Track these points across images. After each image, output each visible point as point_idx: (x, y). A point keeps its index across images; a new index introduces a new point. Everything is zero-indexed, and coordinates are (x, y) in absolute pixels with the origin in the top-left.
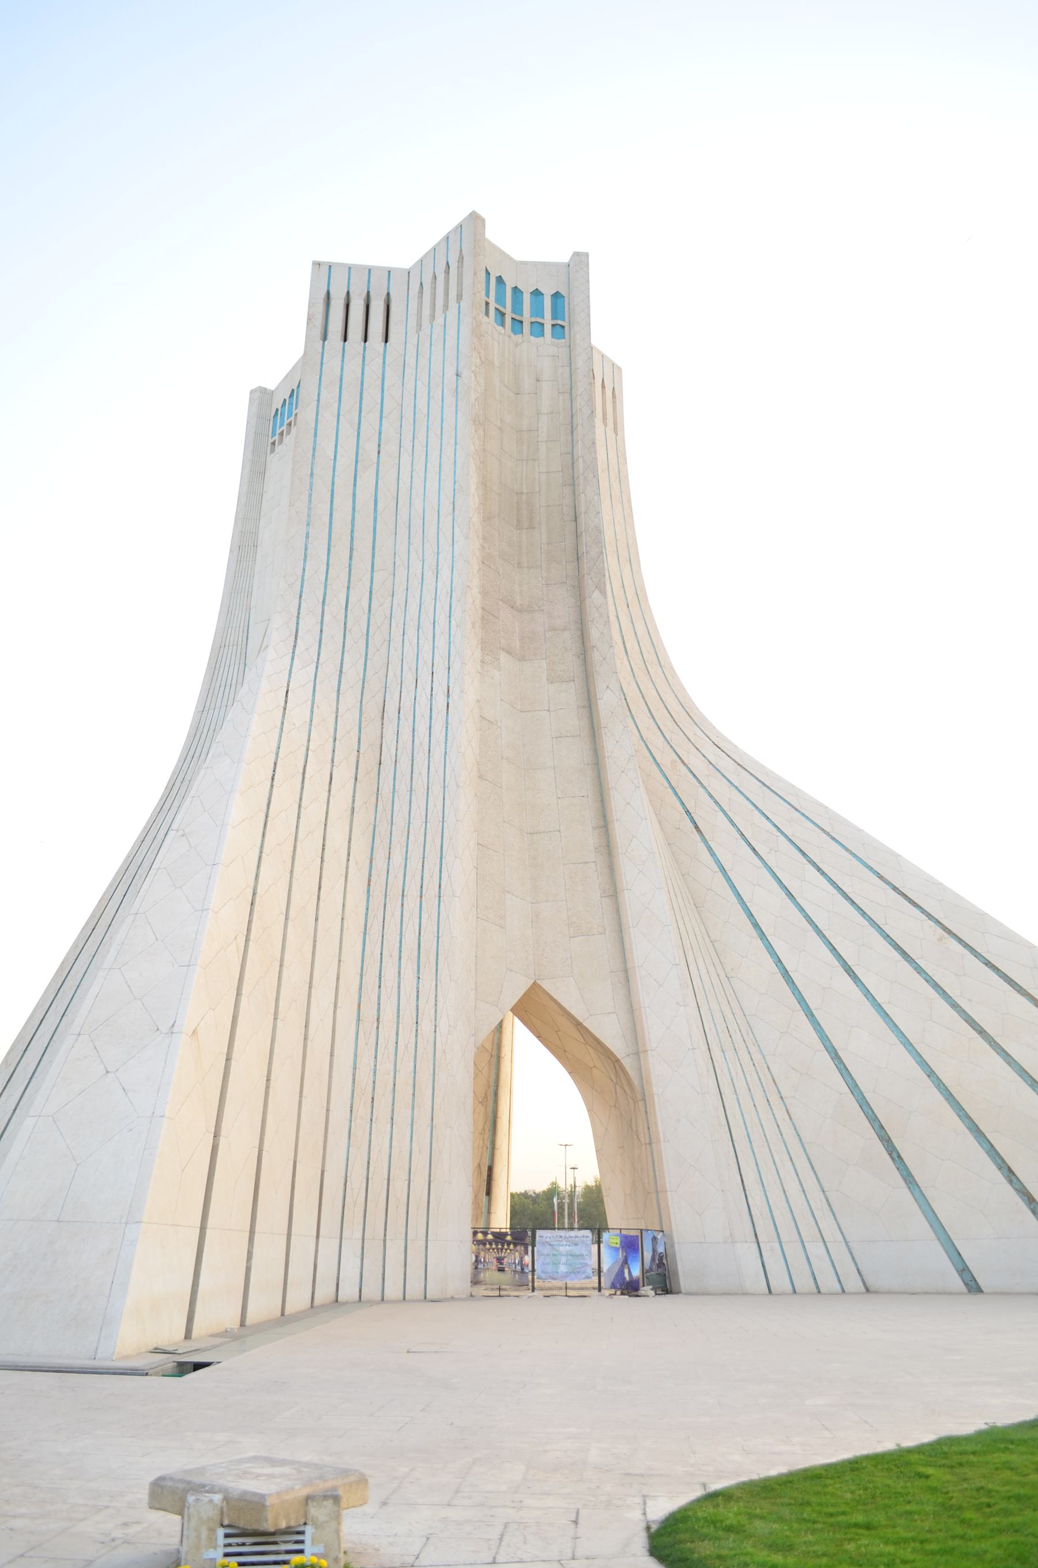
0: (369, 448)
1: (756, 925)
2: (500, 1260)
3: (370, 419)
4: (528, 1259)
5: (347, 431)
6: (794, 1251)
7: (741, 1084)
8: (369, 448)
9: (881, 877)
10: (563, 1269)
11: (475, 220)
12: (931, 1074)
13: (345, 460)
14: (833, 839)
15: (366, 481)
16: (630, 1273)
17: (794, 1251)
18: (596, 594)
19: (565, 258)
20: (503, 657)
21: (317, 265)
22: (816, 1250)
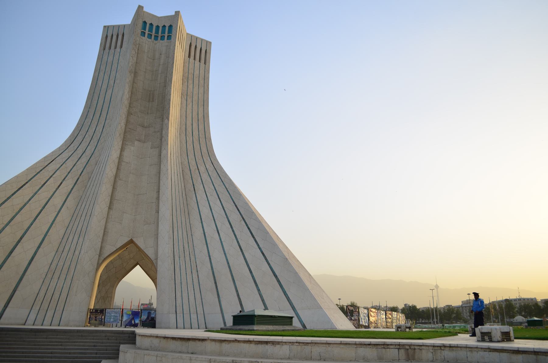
0: (112, 82)
1: (201, 219)
2: (96, 317)
3: (113, 73)
4: (103, 317)
5: (106, 77)
6: (187, 317)
7: (183, 268)
8: (112, 82)
9: (234, 202)
10: (112, 320)
11: (140, 8)
12: (228, 263)
13: (104, 87)
14: (228, 191)
15: (109, 92)
16: (134, 322)
17: (187, 317)
18: (167, 120)
19: (173, 14)
20: (136, 143)
21: (105, 27)
22: (194, 316)
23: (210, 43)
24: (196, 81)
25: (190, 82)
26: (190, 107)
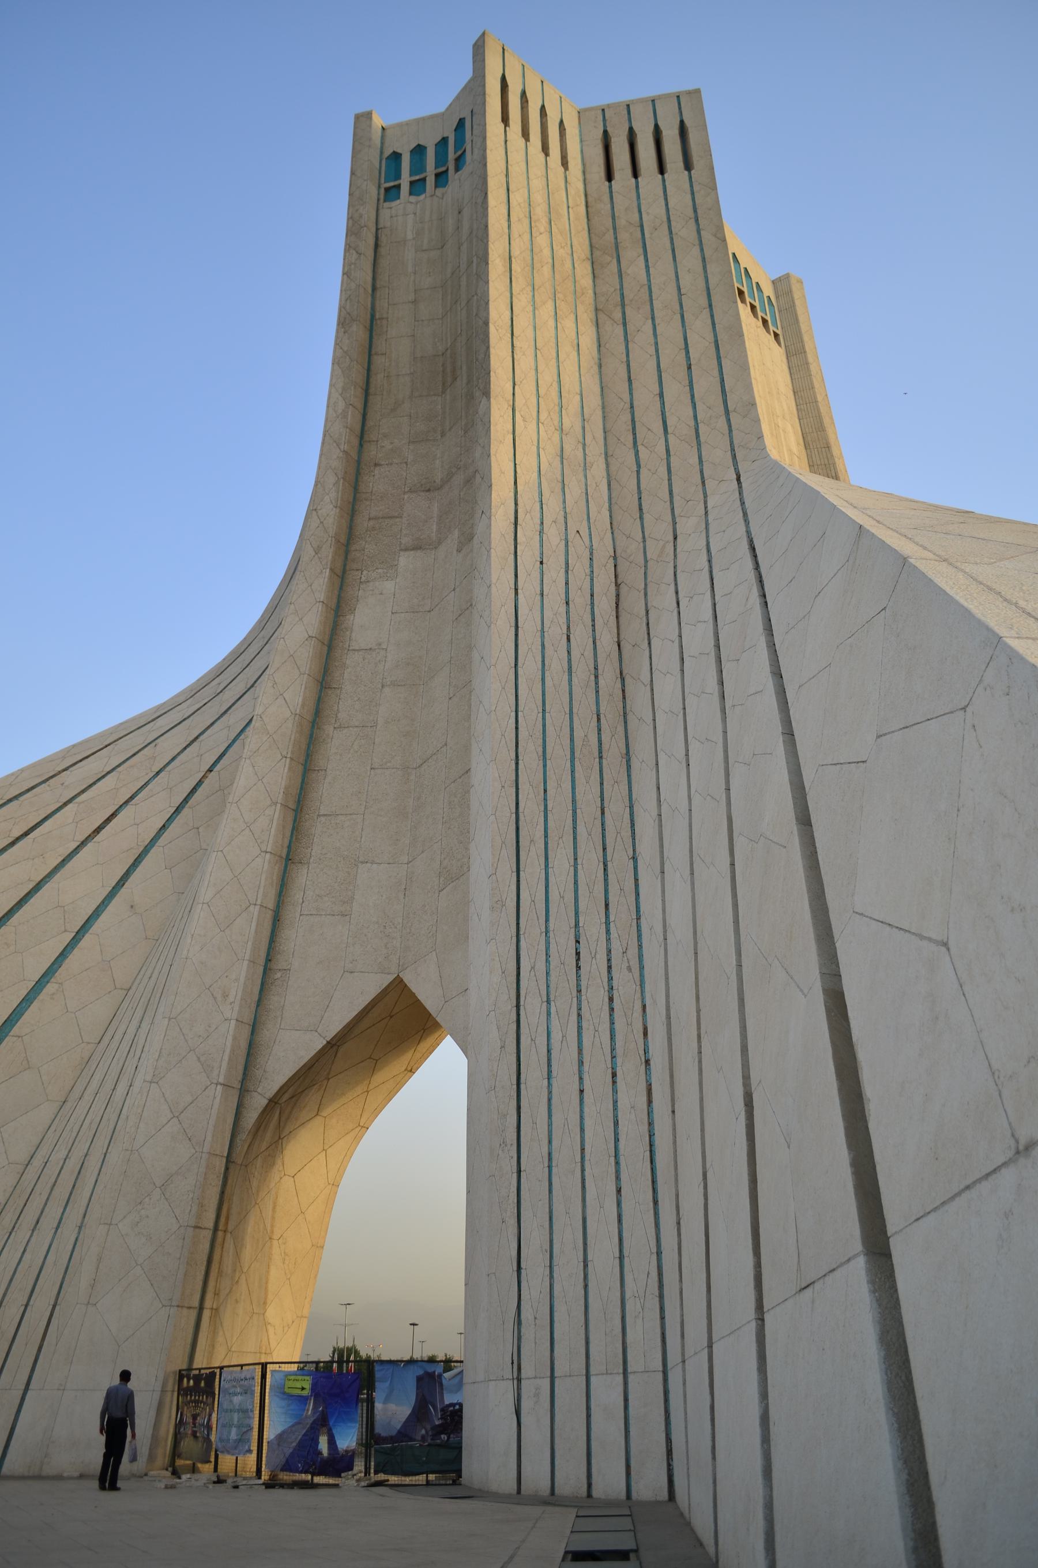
11: (363, 119)
16: (332, 1442)
18: (484, 400)
20: (404, 560)
22: (607, 1392)
23: (698, 92)
24: (658, 243)
25: (631, 254)
26: (642, 339)
